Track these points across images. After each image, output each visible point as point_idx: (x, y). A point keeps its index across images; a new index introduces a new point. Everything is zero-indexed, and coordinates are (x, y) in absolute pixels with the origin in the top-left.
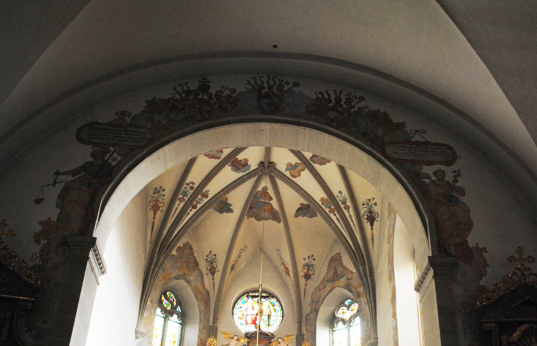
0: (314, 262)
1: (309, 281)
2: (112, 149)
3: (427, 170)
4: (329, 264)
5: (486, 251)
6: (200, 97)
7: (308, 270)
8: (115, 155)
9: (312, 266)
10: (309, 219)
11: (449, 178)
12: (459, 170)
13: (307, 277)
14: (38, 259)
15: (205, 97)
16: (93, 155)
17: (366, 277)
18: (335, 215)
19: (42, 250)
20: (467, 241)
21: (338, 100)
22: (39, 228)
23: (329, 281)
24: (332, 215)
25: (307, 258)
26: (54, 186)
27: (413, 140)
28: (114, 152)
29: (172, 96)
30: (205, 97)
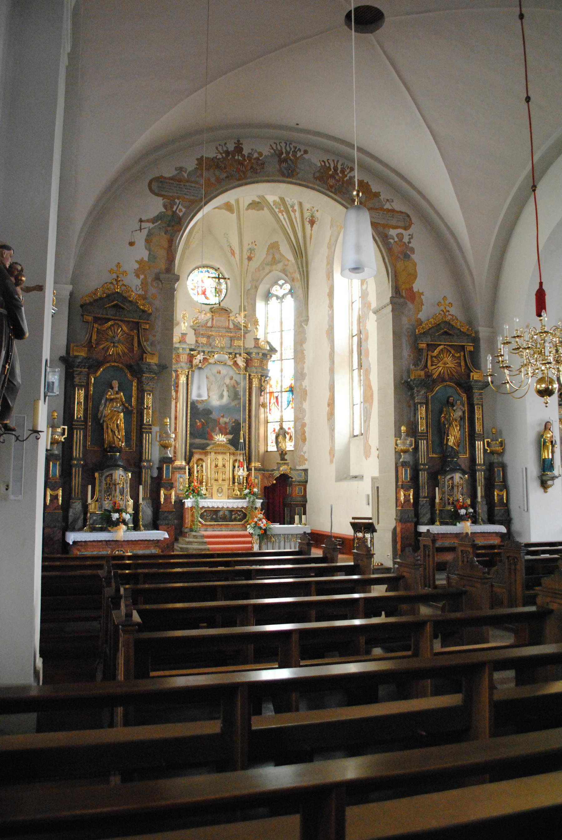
0: (255, 247)
1: (251, 262)
2: (177, 201)
3: (393, 232)
4: (268, 249)
5: (423, 295)
6: (236, 157)
7: (251, 253)
8: (180, 207)
9: (254, 250)
10: (256, 211)
11: (406, 240)
12: (413, 234)
13: (250, 259)
14: (141, 290)
15: (240, 158)
16: (165, 206)
17: (303, 267)
18: (283, 215)
19: (142, 283)
20: (412, 287)
21: (336, 169)
22: (136, 266)
23: (267, 264)
24: (280, 215)
25: (250, 243)
26: (141, 232)
27: (385, 207)
28: (179, 204)
29: (215, 156)
30: (240, 158)
